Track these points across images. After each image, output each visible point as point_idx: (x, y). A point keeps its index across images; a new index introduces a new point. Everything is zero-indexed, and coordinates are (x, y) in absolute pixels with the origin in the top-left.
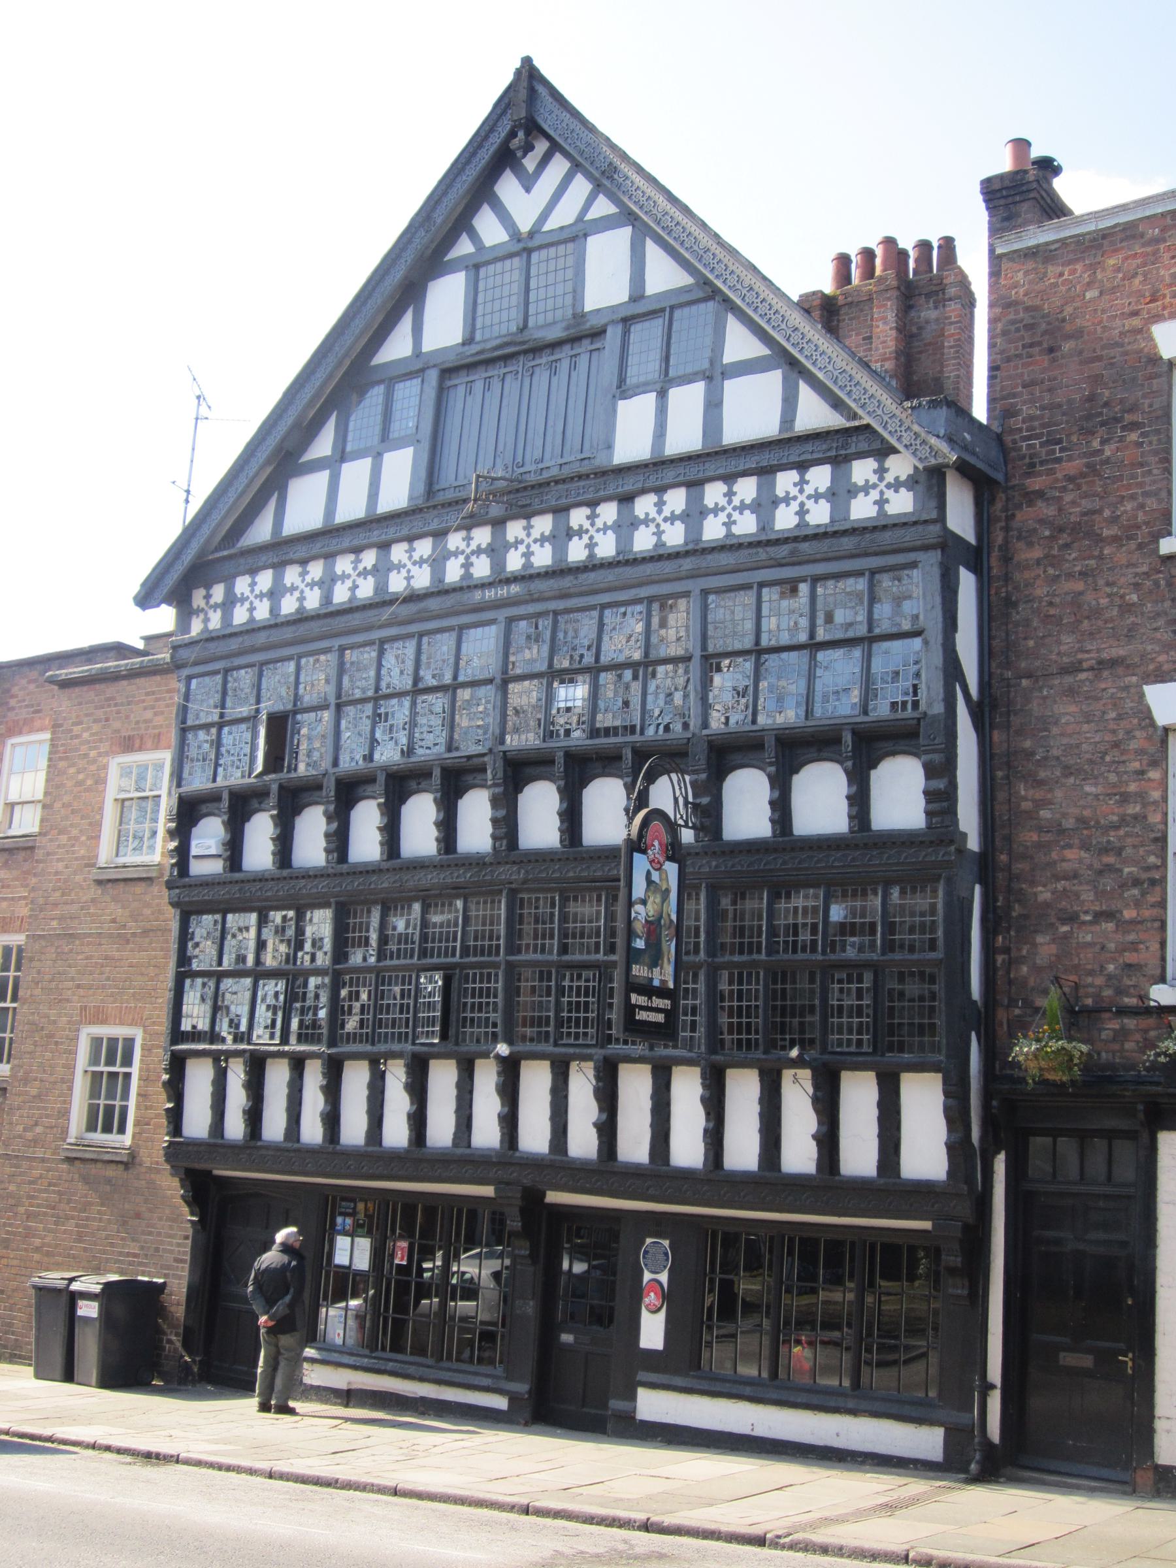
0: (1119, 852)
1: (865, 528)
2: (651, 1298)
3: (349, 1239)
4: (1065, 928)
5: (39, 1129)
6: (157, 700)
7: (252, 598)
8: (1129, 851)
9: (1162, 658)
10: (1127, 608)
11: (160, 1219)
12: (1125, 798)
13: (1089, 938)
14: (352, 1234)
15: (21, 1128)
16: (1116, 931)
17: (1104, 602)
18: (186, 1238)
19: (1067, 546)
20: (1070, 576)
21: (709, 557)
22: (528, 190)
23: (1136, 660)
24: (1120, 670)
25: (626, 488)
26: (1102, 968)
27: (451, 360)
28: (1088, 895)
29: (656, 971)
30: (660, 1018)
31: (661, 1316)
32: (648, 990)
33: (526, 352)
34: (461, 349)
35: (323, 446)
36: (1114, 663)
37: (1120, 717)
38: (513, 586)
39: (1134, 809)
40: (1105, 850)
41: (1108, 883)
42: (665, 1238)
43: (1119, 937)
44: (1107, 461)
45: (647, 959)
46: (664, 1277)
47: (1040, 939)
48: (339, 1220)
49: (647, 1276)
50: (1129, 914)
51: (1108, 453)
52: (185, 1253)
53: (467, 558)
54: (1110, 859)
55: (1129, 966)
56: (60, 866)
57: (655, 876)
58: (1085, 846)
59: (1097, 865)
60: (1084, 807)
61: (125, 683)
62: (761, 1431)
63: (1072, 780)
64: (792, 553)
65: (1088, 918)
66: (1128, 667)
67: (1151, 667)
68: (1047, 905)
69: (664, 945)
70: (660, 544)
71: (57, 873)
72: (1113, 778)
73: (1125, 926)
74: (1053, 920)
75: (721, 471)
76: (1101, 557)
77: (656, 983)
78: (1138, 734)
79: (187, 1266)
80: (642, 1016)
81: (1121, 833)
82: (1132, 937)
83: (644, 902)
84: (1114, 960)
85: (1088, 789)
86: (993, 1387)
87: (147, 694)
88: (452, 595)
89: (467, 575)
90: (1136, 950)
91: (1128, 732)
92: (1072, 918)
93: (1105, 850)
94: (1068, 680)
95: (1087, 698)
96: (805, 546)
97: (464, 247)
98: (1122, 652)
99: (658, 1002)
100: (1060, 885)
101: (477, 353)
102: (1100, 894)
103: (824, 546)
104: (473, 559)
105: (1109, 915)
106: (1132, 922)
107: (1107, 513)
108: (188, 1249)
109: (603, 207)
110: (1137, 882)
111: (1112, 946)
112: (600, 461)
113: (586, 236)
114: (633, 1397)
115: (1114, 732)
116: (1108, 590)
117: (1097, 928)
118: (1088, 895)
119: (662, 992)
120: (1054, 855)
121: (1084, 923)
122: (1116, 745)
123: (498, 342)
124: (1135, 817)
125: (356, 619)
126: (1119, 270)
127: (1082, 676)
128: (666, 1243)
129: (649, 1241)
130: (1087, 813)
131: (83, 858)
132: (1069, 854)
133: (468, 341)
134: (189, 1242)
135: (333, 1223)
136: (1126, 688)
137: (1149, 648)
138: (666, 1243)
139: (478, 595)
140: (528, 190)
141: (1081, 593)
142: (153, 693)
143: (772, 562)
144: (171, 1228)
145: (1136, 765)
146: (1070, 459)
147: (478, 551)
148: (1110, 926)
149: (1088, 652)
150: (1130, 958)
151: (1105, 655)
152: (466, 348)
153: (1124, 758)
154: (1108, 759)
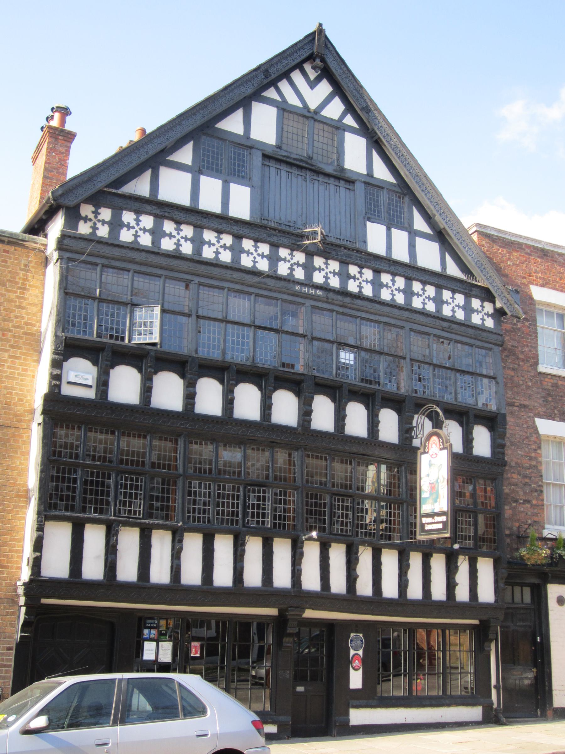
0: (530, 478)
1: (478, 328)
2: (357, 663)
3: (154, 644)
4: (514, 504)
7: (178, 237)
8: (533, 478)
9: (540, 409)
10: (528, 387)
12: (531, 459)
13: (522, 509)
14: (157, 641)
16: (531, 507)
17: (521, 382)
18: (10, 649)
19: (507, 356)
20: (509, 368)
21: (415, 315)
22: (312, 88)
23: (532, 407)
24: (527, 410)
25: (379, 267)
26: (527, 521)
27: (269, 152)
28: (521, 493)
31: (360, 672)
33: (310, 170)
34: (275, 149)
36: (525, 406)
37: (528, 427)
38: (318, 291)
39: (534, 463)
40: (525, 476)
41: (527, 489)
42: (360, 633)
43: (531, 510)
44: (519, 329)
45: (430, 501)
46: (361, 652)
47: (506, 507)
48: (146, 631)
49: (352, 652)
50: (534, 502)
51: (519, 326)
52: (8, 660)
53: (292, 265)
54: (527, 480)
55: (535, 522)
58: (519, 474)
59: (523, 482)
60: (518, 459)
62: (410, 721)
63: (513, 447)
64: (450, 327)
65: (522, 502)
66: (529, 409)
67: (537, 412)
68: (508, 494)
72: (527, 450)
73: (533, 506)
74: (510, 501)
75: (422, 278)
76: (518, 365)
78: (534, 435)
79: (12, 670)
80: (428, 527)
81: (530, 471)
82: (536, 511)
84: (530, 519)
85: (519, 452)
86: (495, 687)
88: (282, 282)
89: (291, 274)
90: (537, 516)
91: (531, 434)
92: (516, 501)
93: (525, 476)
94: (511, 408)
95: (518, 417)
96: (454, 326)
97: (271, 93)
98: (527, 403)
99: (437, 519)
100: (512, 487)
101: (285, 156)
102: (525, 493)
105: (528, 502)
106: (535, 505)
107: (520, 349)
108: (13, 657)
109: (349, 120)
110: (536, 491)
111: (529, 513)
113: (344, 130)
114: (347, 714)
115: (526, 432)
116: (522, 378)
117: (524, 506)
118: (521, 493)
120: (509, 475)
121: (520, 503)
122: (527, 437)
123: (297, 157)
124: (534, 466)
125: (216, 271)
126: (518, 258)
127: (515, 408)
128: (361, 635)
129: (352, 635)
130: (519, 461)
132: (515, 476)
133: (279, 147)
134: (13, 652)
135: (140, 634)
136: (529, 417)
137: (536, 404)
138: (361, 635)
139: (298, 287)
140: (312, 88)
141: (513, 376)
143: (441, 328)
145: (533, 447)
146: (507, 323)
148: (529, 506)
149: (517, 400)
150: (535, 518)
151: (522, 402)
152: (278, 150)
153: (530, 443)
154: (525, 442)
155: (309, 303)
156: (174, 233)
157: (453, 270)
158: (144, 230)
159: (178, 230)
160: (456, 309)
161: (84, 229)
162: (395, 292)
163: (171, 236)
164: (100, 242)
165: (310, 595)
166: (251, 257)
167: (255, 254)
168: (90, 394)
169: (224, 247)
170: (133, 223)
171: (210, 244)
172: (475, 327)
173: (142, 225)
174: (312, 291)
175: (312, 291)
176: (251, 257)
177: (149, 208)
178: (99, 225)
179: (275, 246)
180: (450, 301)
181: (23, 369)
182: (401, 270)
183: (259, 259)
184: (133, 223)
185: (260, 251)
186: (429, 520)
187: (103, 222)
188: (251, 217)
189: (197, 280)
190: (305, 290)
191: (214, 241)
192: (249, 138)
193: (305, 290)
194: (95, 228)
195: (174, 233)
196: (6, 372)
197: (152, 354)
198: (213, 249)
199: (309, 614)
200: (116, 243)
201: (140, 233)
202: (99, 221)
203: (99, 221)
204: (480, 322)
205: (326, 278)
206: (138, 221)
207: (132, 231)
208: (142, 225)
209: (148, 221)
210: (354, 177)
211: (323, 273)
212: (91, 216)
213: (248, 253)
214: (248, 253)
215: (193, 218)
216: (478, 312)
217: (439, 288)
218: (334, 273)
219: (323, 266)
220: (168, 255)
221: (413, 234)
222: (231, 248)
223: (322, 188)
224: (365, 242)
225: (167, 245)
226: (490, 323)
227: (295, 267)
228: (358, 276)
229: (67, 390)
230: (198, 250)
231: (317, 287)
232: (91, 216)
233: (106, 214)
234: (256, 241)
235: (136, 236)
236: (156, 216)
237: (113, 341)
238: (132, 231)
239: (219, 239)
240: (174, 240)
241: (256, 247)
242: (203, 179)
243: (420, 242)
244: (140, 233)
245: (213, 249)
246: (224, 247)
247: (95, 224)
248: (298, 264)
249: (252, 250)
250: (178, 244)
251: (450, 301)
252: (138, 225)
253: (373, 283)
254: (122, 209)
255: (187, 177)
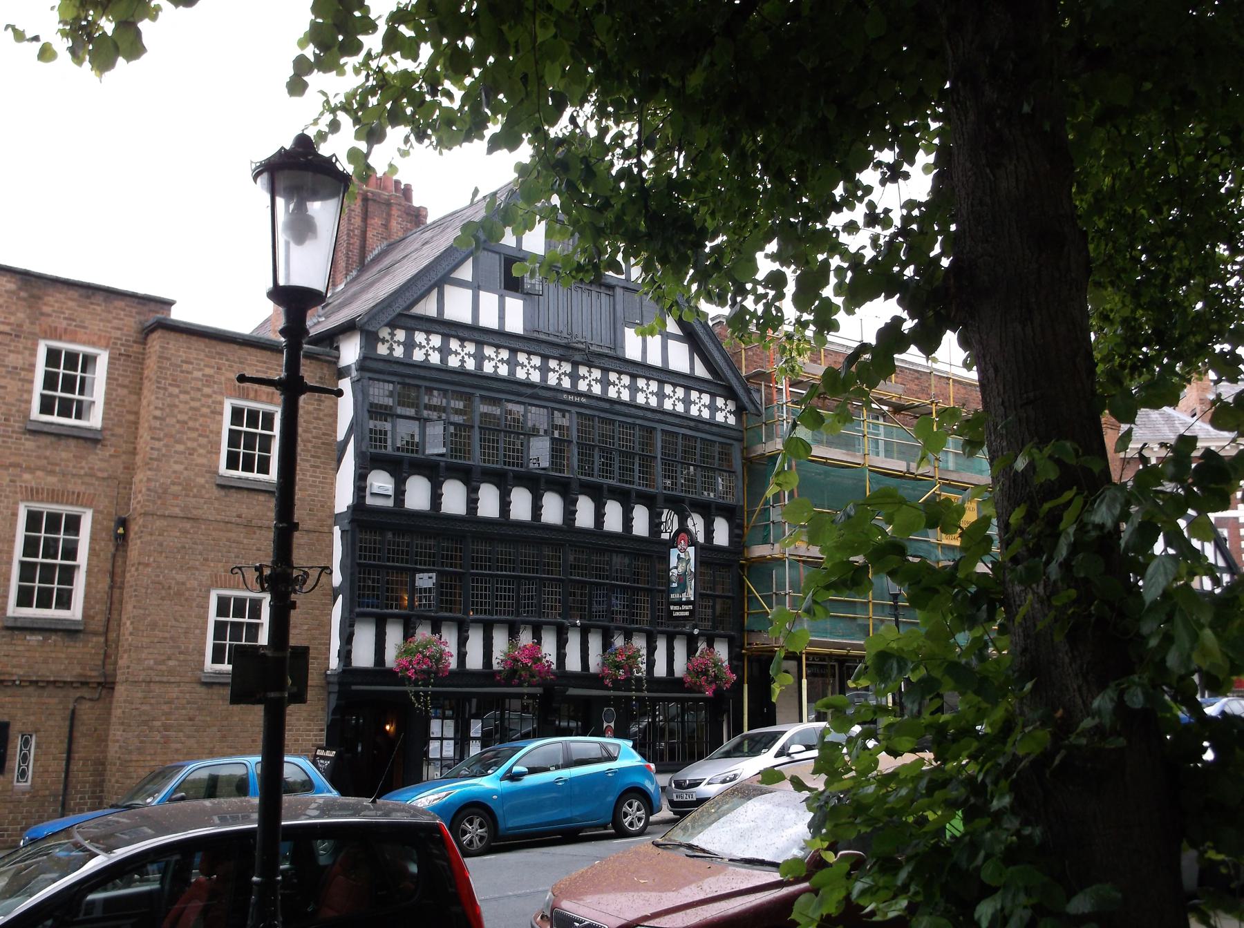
5: (171, 663)
6: (268, 368)
11: (298, 720)
14: (444, 718)
15: (152, 662)
18: (322, 730)
29: (684, 595)
30: (687, 614)
32: (680, 603)
35: (466, 272)
45: (679, 590)
46: (612, 724)
49: (605, 725)
56: (178, 467)
57: (682, 555)
61: (236, 347)
69: (688, 583)
70: (647, 403)
71: (175, 472)
77: (684, 599)
83: (676, 568)
87: (260, 362)
89: (559, 384)
96: (700, 425)
99: (687, 607)
103: (707, 427)
104: (563, 377)
112: (619, 354)
119: (688, 602)
131: (203, 465)
134: (325, 733)
139: (565, 396)
142: (265, 363)
144: (309, 725)
147: (565, 374)
155: (574, 410)
156: (459, 350)
157: (701, 371)
158: (434, 348)
159: (462, 346)
160: (702, 408)
161: (382, 350)
162: (649, 396)
163: (456, 353)
164: (397, 362)
165: (573, 675)
166: (525, 370)
167: (528, 367)
168: (390, 503)
169: (502, 361)
170: (424, 343)
171: (490, 359)
172: (718, 425)
173: (431, 344)
174: (577, 399)
175: (577, 399)
176: (525, 370)
177: (438, 328)
178: (395, 346)
179: (545, 358)
180: (697, 401)
181: (324, 478)
182: (655, 375)
183: (531, 371)
184: (424, 343)
185: (532, 363)
186: (676, 608)
187: (399, 343)
188: (524, 329)
189: (478, 393)
190: (571, 398)
191: (493, 355)
192: (521, 249)
193: (571, 398)
194: (391, 349)
195: (459, 350)
196: (308, 481)
197: (442, 464)
198: (493, 363)
199: (572, 691)
200: (410, 362)
201: (431, 352)
202: (395, 342)
203: (395, 342)
204: (723, 420)
205: (590, 385)
206: (428, 340)
207: (424, 351)
208: (431, 344)
209: (436, 340)
210: (614, 283)
211: (587, 381)
212: (388, 337)
213: (523, 366)
214: (523, 366)
215: (477, 336)
216: (721, 410)
217: (688, 389)
218: (596, 380)
219: (587, 375)
220: (453, 372)
221: (666, 336)
222: (508, 362)
223: (585, 295)
224: (623, 348)
225: (453, 362)
226: (732, 420)
227: (563, 377)
228: (617, 382)
229: (370, 501)
230: (479, 366)
231: (581, 394)
232: (388, 337)
233: (401, 335)
234: (529, 353)
235: (427, 355)
236: (443, 335)
237: (409, 455)
238: (424, 351)
239: (497, 353)
240: (459, 357)
241: (529, 359)
242: (482, 294)
243: (671, 343)
244: (431, 352)
245: (493, 363)
246: (502, 361)
247: (391, 345)
248: (565, 374)
249: (526, 362)
250: (463, 361)
251: (697, 401)
252: (428, 344)
253: (629, 387)
254: (415, 329)
255: (468, 293)
